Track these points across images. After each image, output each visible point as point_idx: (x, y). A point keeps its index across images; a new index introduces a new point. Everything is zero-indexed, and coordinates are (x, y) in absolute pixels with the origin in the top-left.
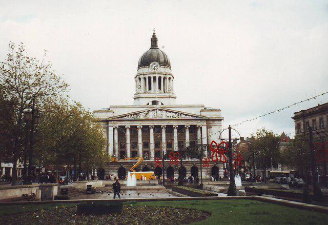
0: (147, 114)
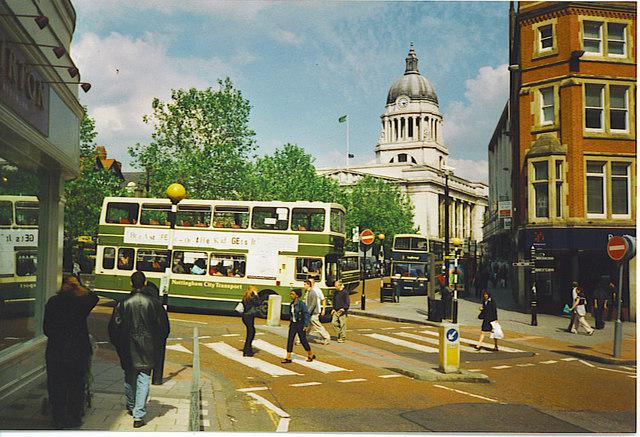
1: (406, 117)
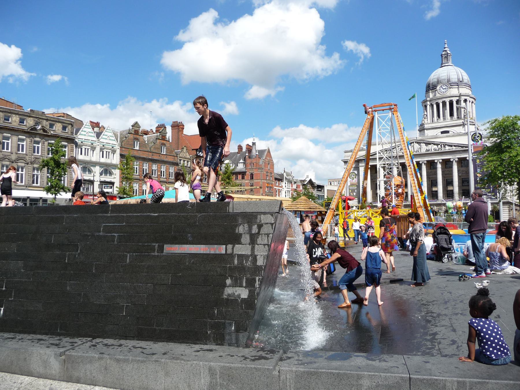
1: (447, 100)
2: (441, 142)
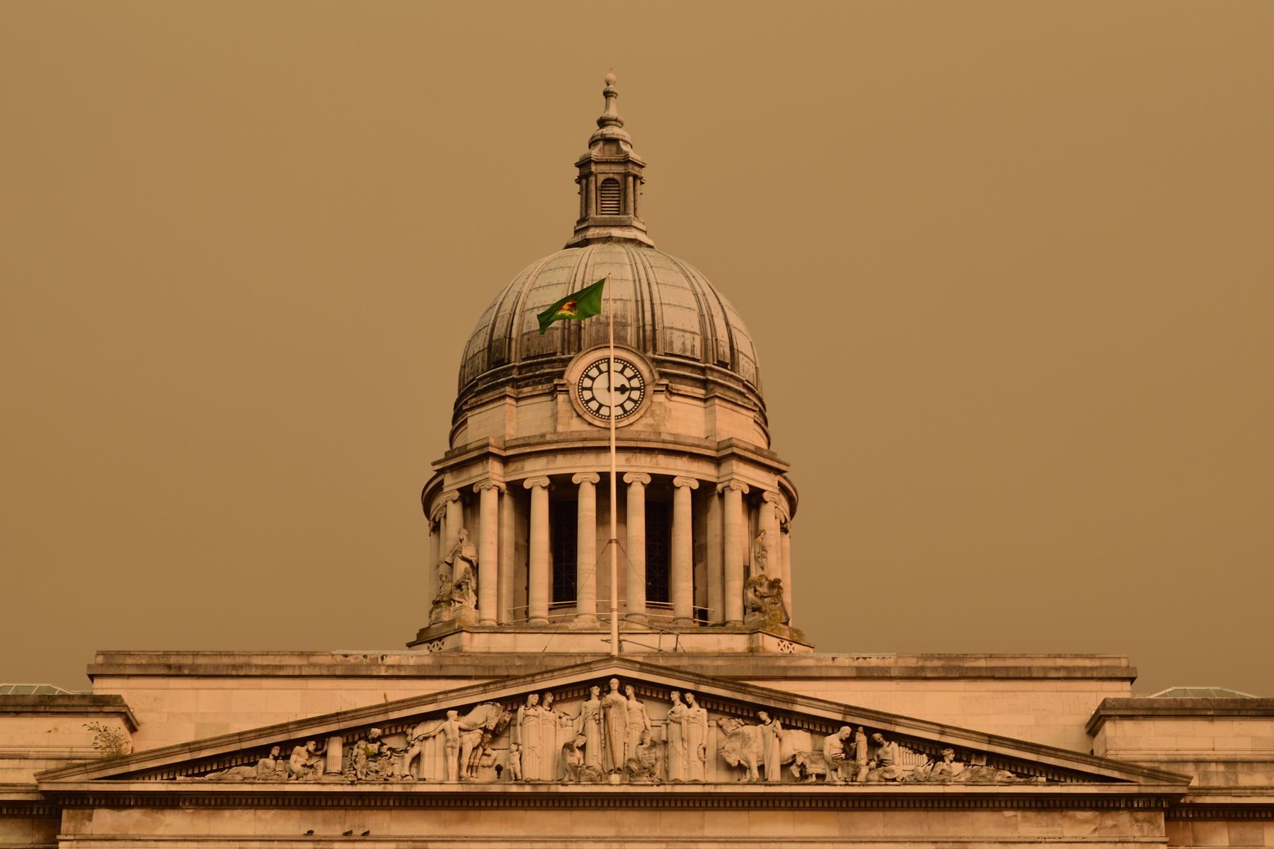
0: (494, 734)
1: (639, 470)
2: (849, 710)
